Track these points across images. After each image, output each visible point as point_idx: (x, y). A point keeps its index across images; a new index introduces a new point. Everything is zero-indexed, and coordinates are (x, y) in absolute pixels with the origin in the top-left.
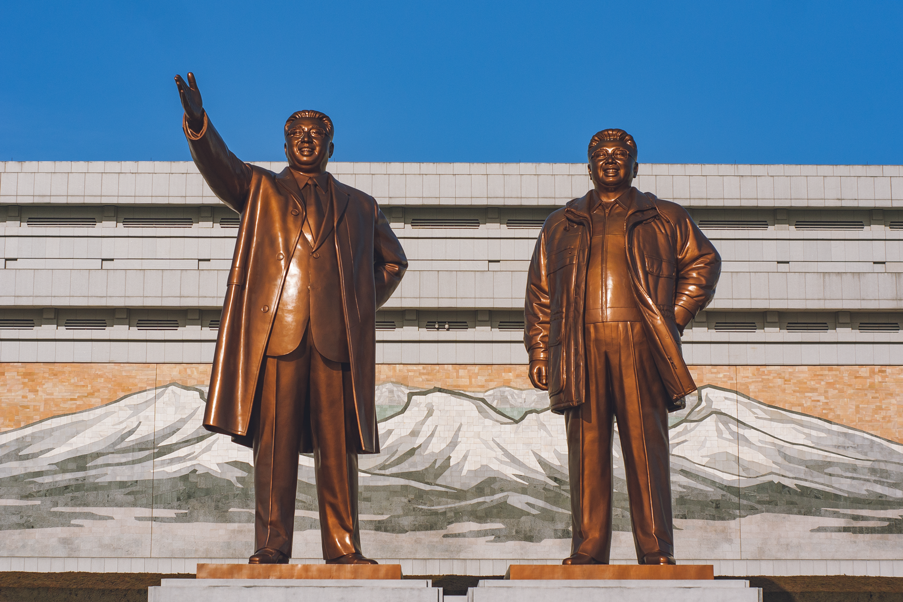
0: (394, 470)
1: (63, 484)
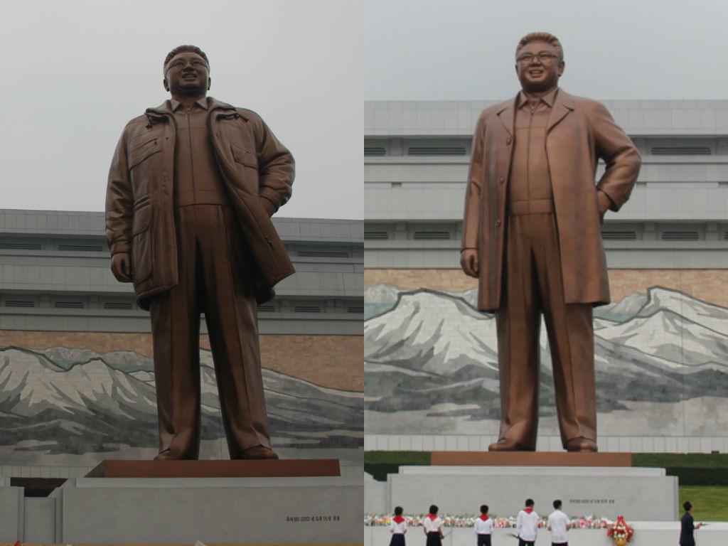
0: (387, 358)
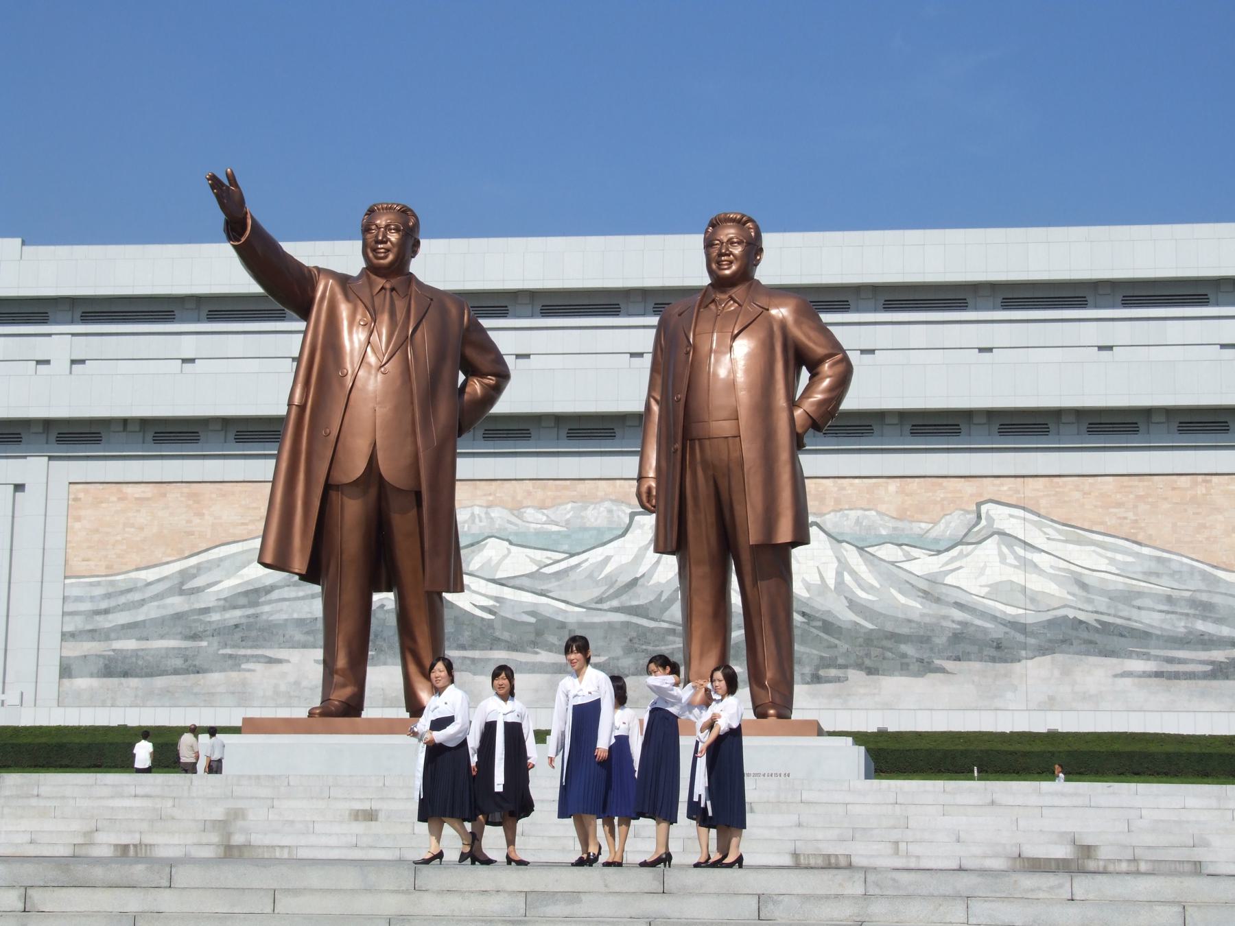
0: (615, 603)
1: (232, 623)
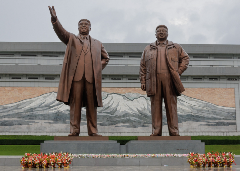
0: (104, 111)
1: (28, 115)
